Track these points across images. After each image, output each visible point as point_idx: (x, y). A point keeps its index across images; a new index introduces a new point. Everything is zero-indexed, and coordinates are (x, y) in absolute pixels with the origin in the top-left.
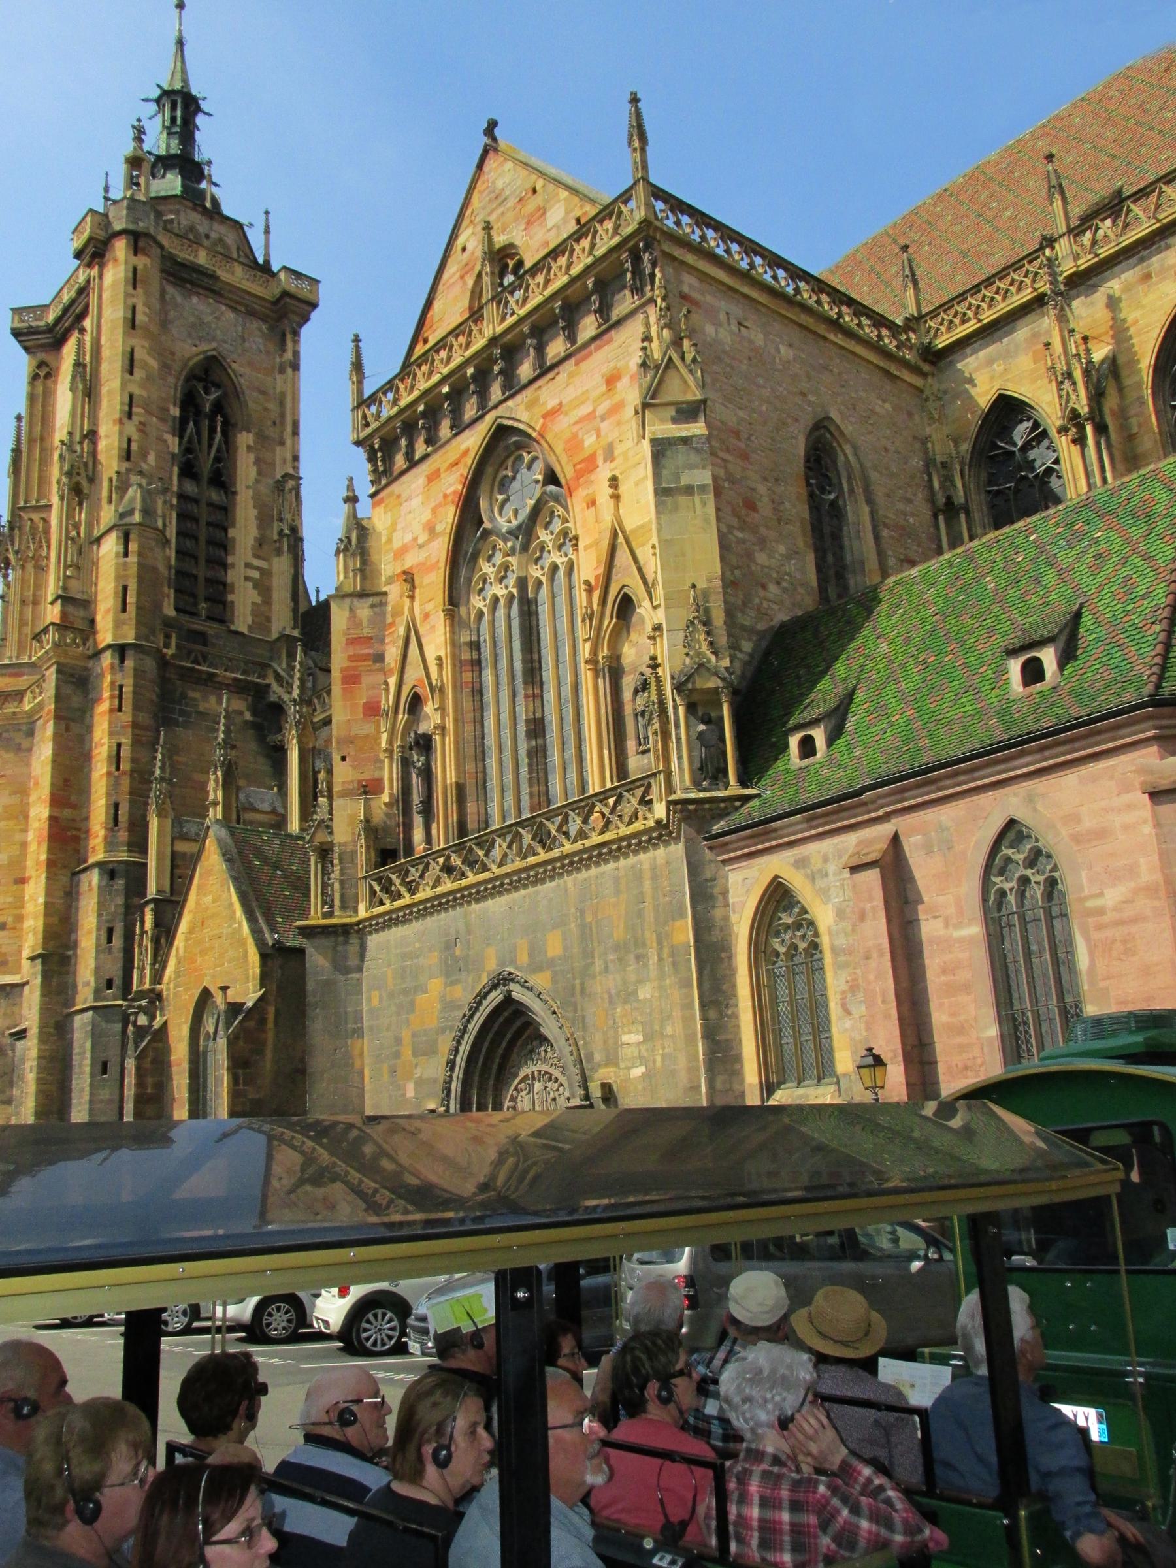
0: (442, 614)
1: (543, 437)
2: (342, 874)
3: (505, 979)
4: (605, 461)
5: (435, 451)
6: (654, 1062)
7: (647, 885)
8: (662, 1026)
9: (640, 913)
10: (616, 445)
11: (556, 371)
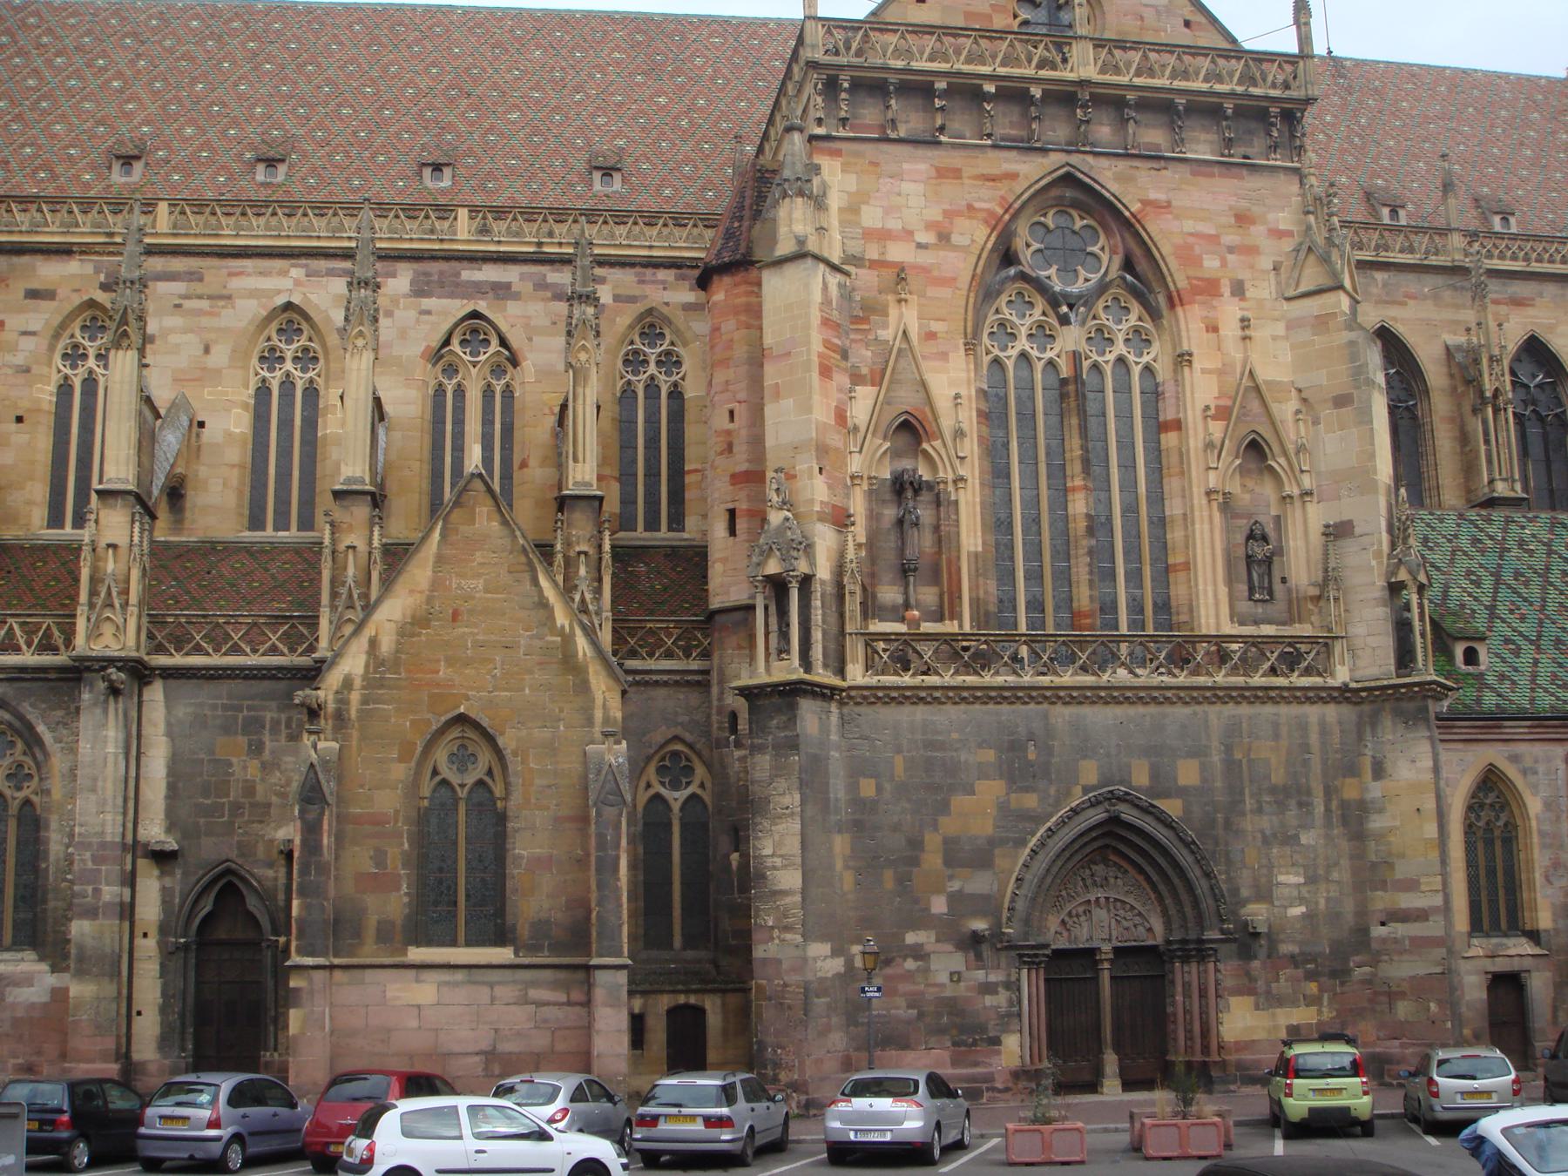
0: (962, 348)
1: (1138, 221)
2: (824, 621)
3: (1118, 799)
4: (1233, 294)
5: (954, 145)
6: (1317, 903)
7: (1314, 738)
8: (1328, 868)
9: (1306, 763)
10: (1247, 285)
11: (1163, 163)
